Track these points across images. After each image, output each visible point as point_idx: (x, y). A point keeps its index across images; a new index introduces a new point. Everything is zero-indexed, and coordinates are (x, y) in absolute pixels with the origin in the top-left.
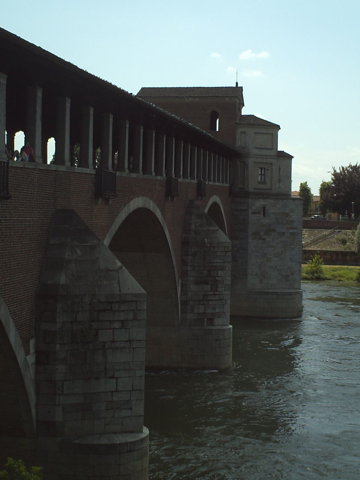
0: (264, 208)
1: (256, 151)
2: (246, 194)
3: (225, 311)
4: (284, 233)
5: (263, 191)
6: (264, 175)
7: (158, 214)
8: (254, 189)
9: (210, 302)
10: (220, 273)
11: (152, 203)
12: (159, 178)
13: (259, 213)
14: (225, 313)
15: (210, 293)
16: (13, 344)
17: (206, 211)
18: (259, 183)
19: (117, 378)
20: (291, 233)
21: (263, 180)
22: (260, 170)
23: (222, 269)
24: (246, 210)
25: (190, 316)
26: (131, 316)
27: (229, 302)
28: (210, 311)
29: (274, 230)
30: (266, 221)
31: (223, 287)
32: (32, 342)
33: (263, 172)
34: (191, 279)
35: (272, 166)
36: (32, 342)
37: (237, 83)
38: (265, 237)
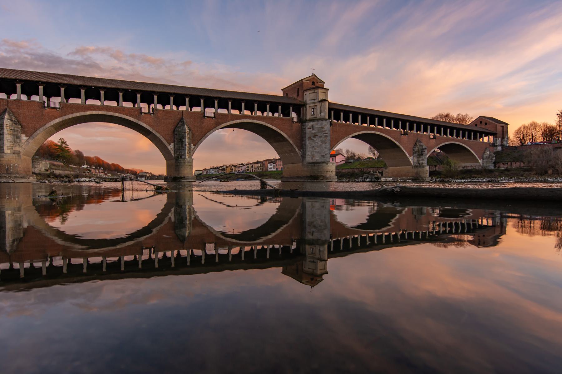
0: (313, 126)
1: (310, 102)
4: (322, 136)
5: (313, 118)
6: (314, 111)
9: (181, 150)
13: (310, 128)
20: (325, 136)
22: (313, 109)
23: (184, 139)
25: (176, 155)
28: (180, 153)
29: (317, 135)
30: (314, 131)
37: (313, 74)
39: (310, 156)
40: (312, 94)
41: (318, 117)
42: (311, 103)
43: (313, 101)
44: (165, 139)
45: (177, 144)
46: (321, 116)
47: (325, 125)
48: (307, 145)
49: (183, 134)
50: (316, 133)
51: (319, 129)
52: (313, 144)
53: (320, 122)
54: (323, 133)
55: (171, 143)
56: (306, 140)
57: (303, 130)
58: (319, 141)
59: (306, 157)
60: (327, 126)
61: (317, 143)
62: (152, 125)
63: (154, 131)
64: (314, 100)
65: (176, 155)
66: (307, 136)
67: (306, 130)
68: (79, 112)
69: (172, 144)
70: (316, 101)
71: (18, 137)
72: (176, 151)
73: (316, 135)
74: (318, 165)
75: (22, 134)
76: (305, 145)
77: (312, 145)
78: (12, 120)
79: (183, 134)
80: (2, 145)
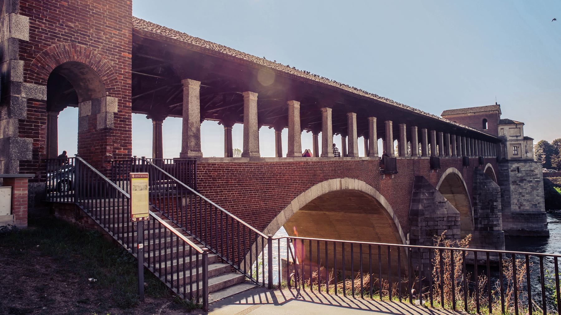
2: (506, 161)
4: (531, 181)
6: (517, 150)
7: (460, 175)
8: (511, 158)
9: (490, 219)
10: (495, 204)
11: (456, 170)
12: (459, 157)
13: (515, 171)
14: (499, 224)
15: (490, 214)
16: (401, 235)
17: (484, 172)
18: (514, 154)
20: (536, 181)
21: (516, 153)
23: (495, 202)
24: (507, 170)
25: (479, 226)
26: (453, 224)
27: (501, 218)
29: (525, 180)
30: (520, 175)
32: (408, 235)
33: (516, 149)
34: (479, 207)
35: (521, 145)
36: (408, 235)
37: (496, 103)
38: (520, 183)
39: (516, 204)
40: (513, 129)
41: (524, 157)
42: (512, 140)
43: (515, 138)
45: (482, 209)
46: (526, 156)
47: (536, 168)
48: (511, 191)
50: (524, 176)
51: (527, 172)
52: (521, 191)
53: (528, 165)
54: (534, 177)
56: (509, 184)
57: (501, 171)
58: (528, 187)
59: (510, 206)
60: (538, 169)
61: (526, 189)
64: (517, 136)
66: (511, 179)
67: (508, 172)
70: (519, 138)
72: (480, 219)
73: (524, 178)
74: (537, 217)
76: (509, 191)
77: (518, 192)
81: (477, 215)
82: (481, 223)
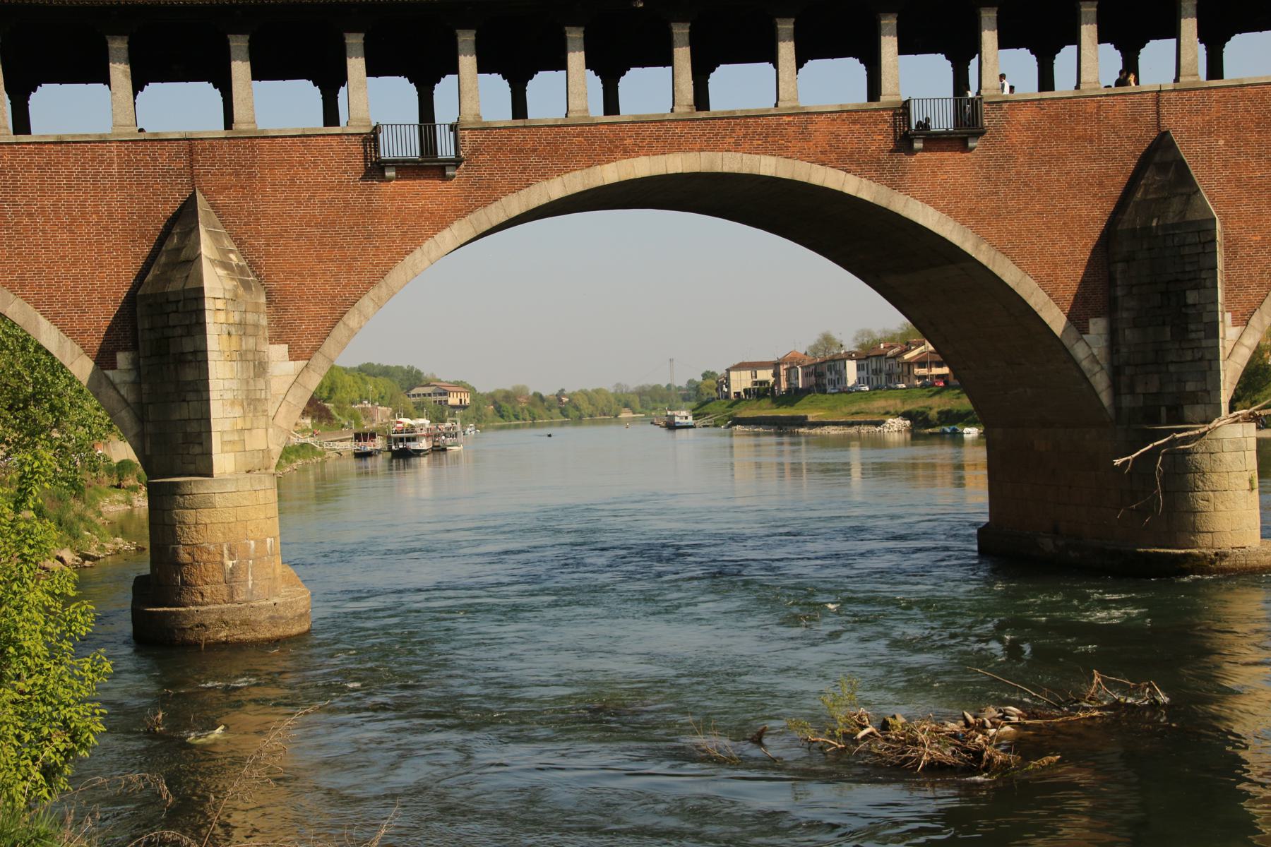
3: (1209, 388)
9: (1172, 368)
19: (188, 402)
23: (1196, 288)
25: (1127, 401)
31: (1201, 331)
34: (1125, 315)
44: (1050, 295)
49: (1187, 251)
55: (1092, 321)
62: (971, 212)
63: (984, 247)
65: (1127, 401)
68: (564, 170)
69: (1098, 326)
71: (260, 368)
72: (1128, 371)
75: (276, 338)
78: (226, 265)
79: (1187, 251)
80: (193, 428)
81: (1118, 351)
82: (1132, 391)
